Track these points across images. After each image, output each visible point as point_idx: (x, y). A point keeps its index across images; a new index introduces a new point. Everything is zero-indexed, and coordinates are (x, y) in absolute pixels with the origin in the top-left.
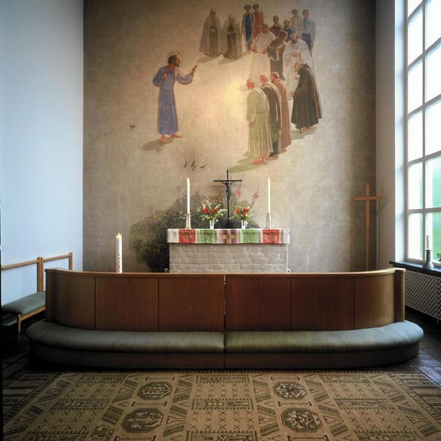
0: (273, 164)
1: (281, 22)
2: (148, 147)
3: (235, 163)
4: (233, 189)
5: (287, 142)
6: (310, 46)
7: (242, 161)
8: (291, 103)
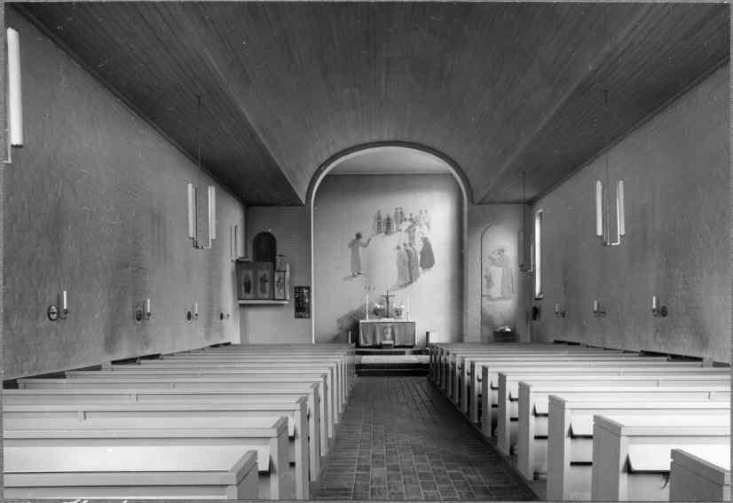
0: (410, 287)
1: (414, 216)
2: (345, 279)
3: (390, 287)
4: (390, 299)
5: (418, 275)
6: (429, 228)
7: (394, 286)
8: (419, 257)
